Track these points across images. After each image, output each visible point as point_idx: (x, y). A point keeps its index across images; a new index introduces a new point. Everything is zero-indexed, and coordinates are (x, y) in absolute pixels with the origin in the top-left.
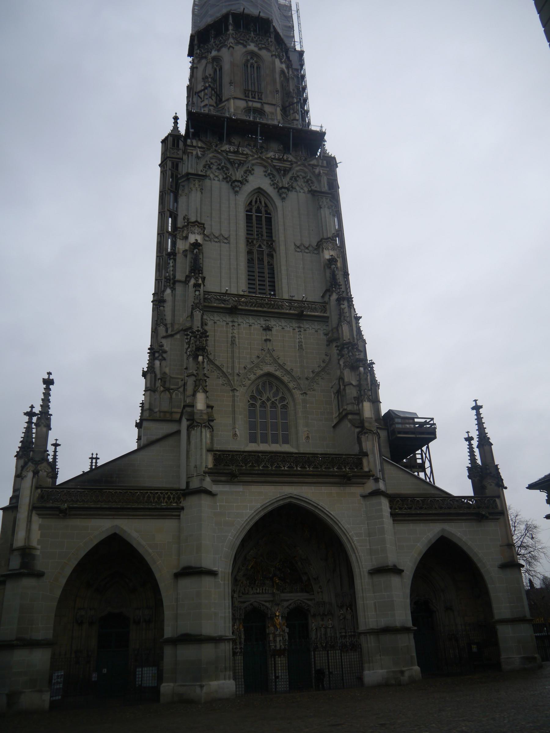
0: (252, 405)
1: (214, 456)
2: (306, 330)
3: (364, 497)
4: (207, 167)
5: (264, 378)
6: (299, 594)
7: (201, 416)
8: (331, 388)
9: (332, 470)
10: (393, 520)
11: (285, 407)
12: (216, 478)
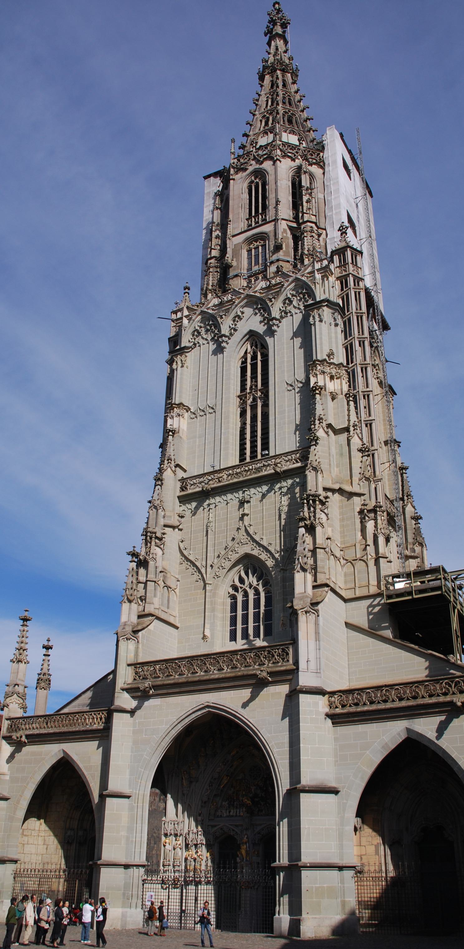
0: (234, 597)
4: (196, 333)
5: (246, 561)
7: (124, 628)
9: (252, 667)
10: (333, 723)
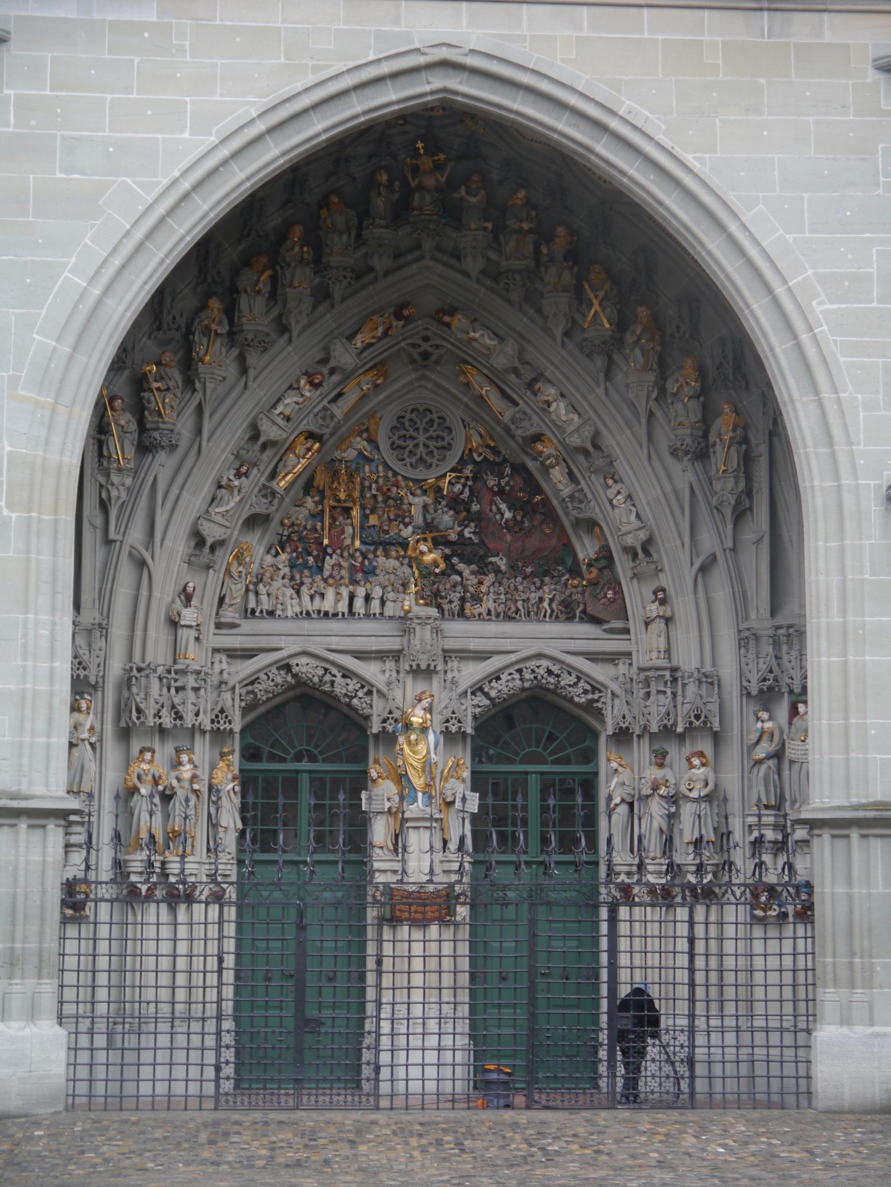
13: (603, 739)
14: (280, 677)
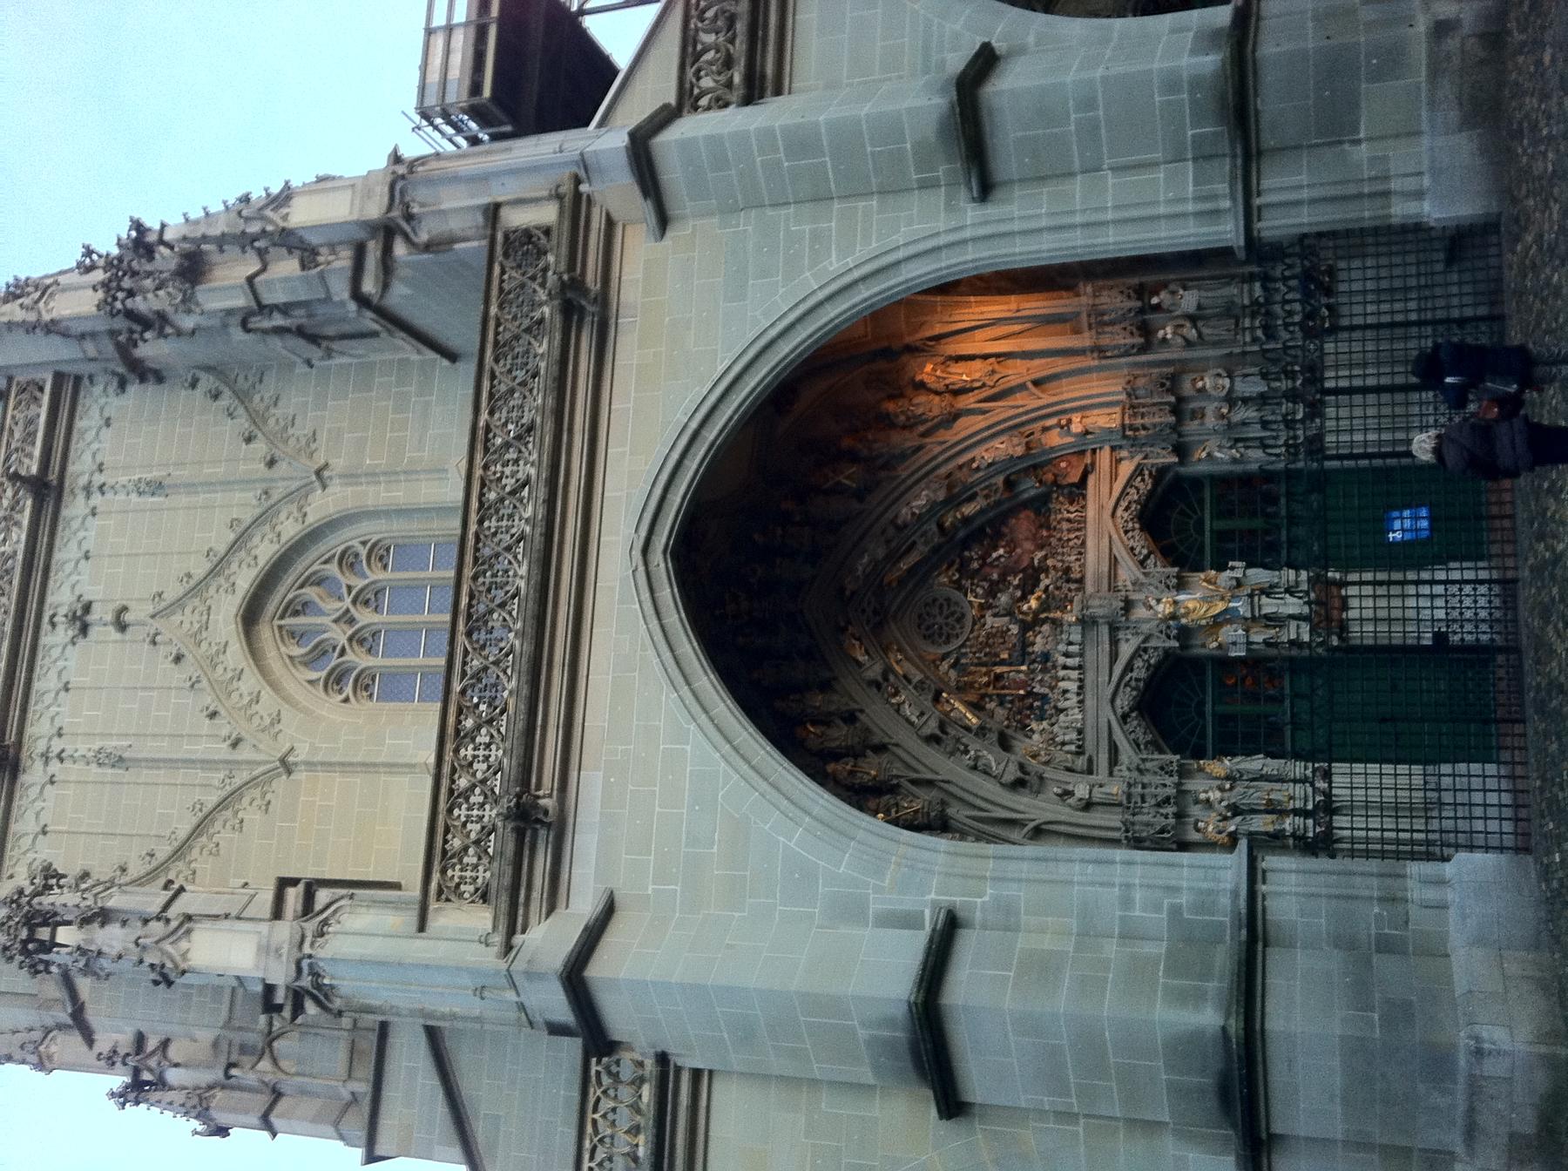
0: (364, 683)
1: (448, 900)
2: (101, 464)
3: (663, 221)
5: (265, 632)
6: (1091, 513)
8: (311, 366)
10: (778, 92)
11: (378, 553)
12: (536, 895)
13: (1182, 470)
14: (1133, 723)
